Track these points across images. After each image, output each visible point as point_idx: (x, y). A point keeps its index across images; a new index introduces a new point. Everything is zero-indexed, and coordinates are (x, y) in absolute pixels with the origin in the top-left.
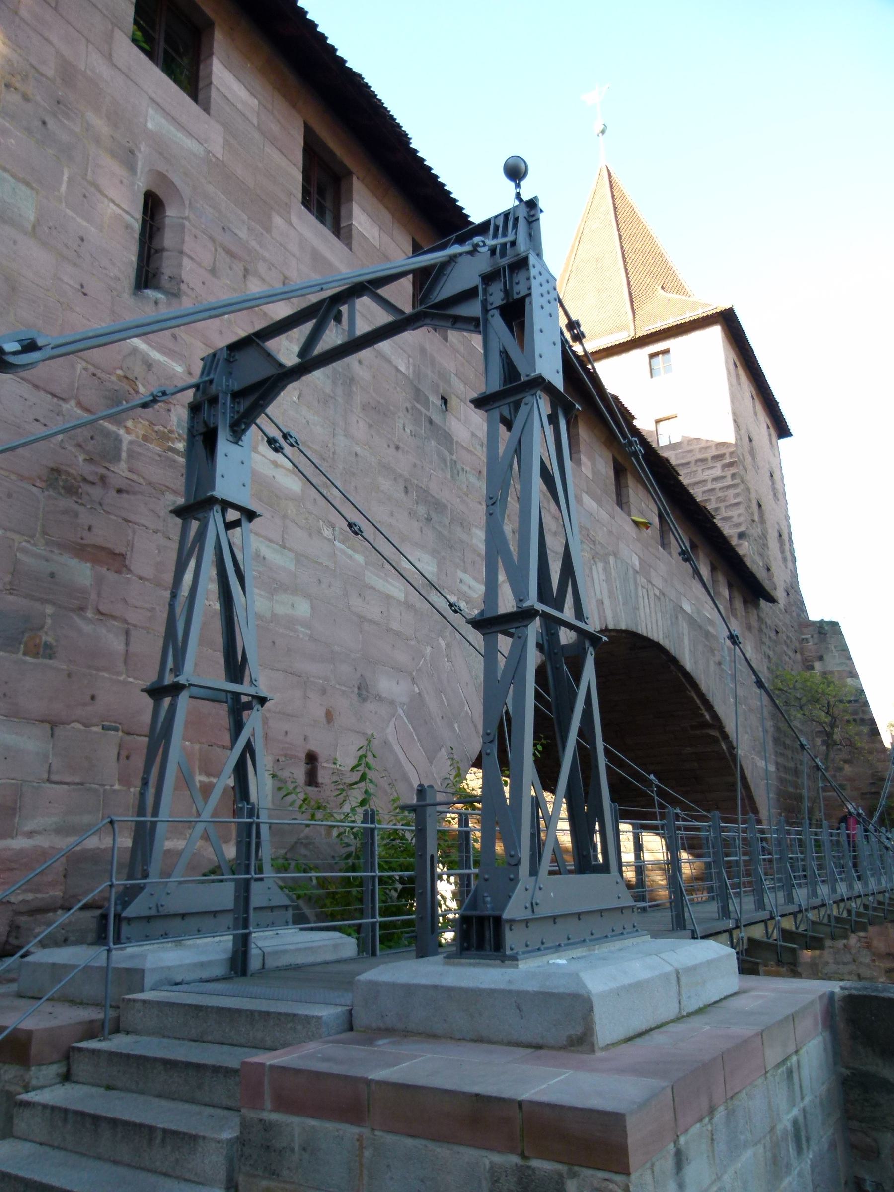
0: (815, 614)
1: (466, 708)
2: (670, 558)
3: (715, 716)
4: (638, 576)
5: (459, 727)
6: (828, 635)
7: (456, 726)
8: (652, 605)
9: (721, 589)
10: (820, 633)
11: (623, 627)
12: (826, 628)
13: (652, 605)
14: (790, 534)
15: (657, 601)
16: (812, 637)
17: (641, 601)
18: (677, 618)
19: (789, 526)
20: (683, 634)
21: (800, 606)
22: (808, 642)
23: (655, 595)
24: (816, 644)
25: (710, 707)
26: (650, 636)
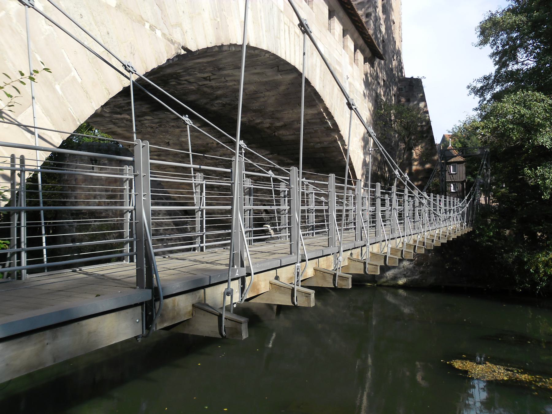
0: (408, 73)
1: (74, 73)
2: (311, 10)
3: (335, 125)
4: (282, 15)
5: (62, 89)
6: (414, 87)
7: (58, 87)
8: (292, 39)
9: (349, 44)
10: (410, 85)
11: (265, 48)
12: (414, 82)
13: (292, 39)
14: (400, 24)
15: (296, 37)
16: (405, 87)
17: (282, 33)
18: (312, 54)
19: (401, 19)
20: (316, 65)
21: (400, 68)
22: (402, 91)
23: (295, 33)
24: (407, 92)
25: (331, 118)
26: (288, 60)
